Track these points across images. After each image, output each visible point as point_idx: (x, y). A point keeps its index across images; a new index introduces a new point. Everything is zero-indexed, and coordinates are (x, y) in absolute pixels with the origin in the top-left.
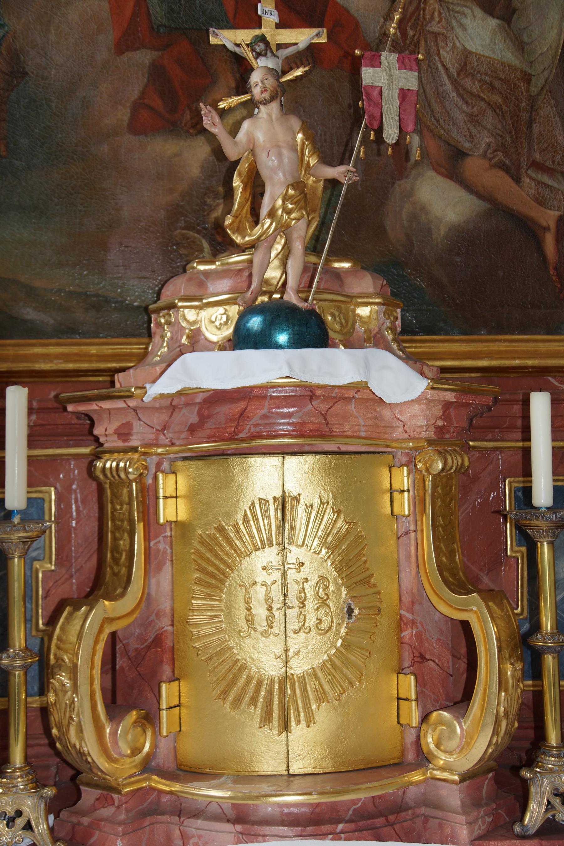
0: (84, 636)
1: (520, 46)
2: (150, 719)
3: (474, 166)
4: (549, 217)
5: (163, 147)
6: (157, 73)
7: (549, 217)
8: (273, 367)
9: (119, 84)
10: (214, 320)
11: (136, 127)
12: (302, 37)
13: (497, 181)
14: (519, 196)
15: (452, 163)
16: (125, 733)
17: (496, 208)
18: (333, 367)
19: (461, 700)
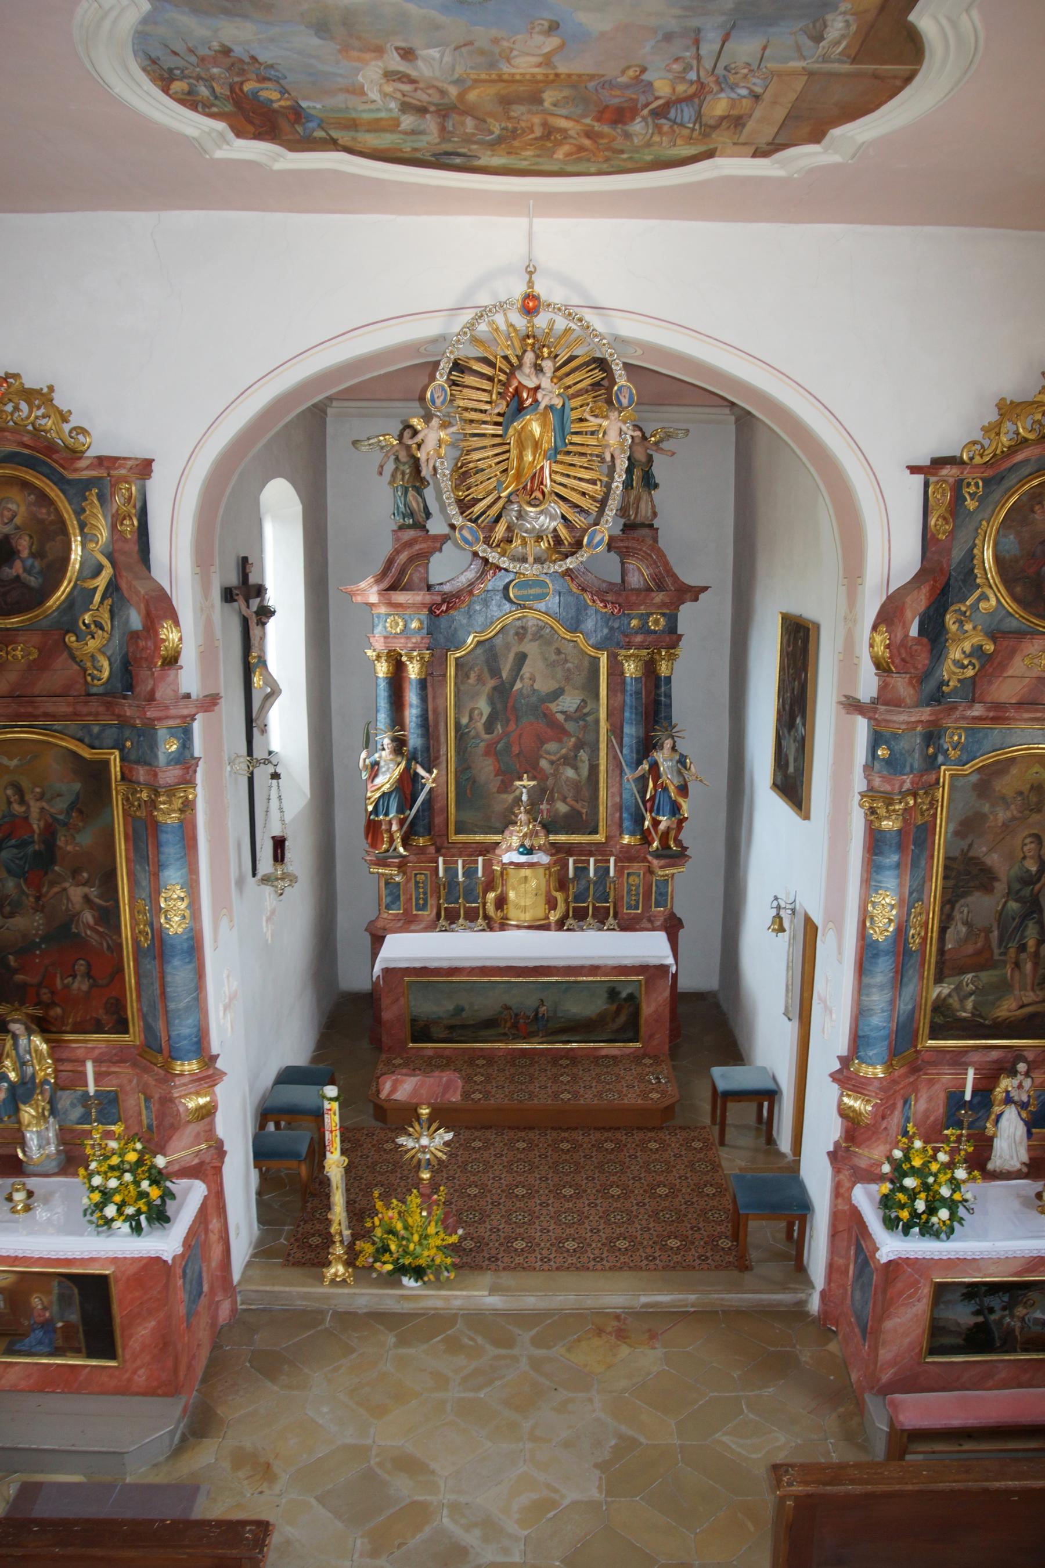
0: (491, 896)
1: (579, 776)
2: (502, 910)
3: (568, 800)
4: (584, 811)
5: (505, 796)
6: (502, 781)
7: (584, 811)
8: (523, 859)
9: (494, 784)
10: (515, 841)
11: (498, 792)
12: (532, 783)
13: (573, 803)
14: (578, 806)
15: (564, 800)
16: (499, 913)
17: (573, 809)
18: (534, 858)
19: (555, 909)
